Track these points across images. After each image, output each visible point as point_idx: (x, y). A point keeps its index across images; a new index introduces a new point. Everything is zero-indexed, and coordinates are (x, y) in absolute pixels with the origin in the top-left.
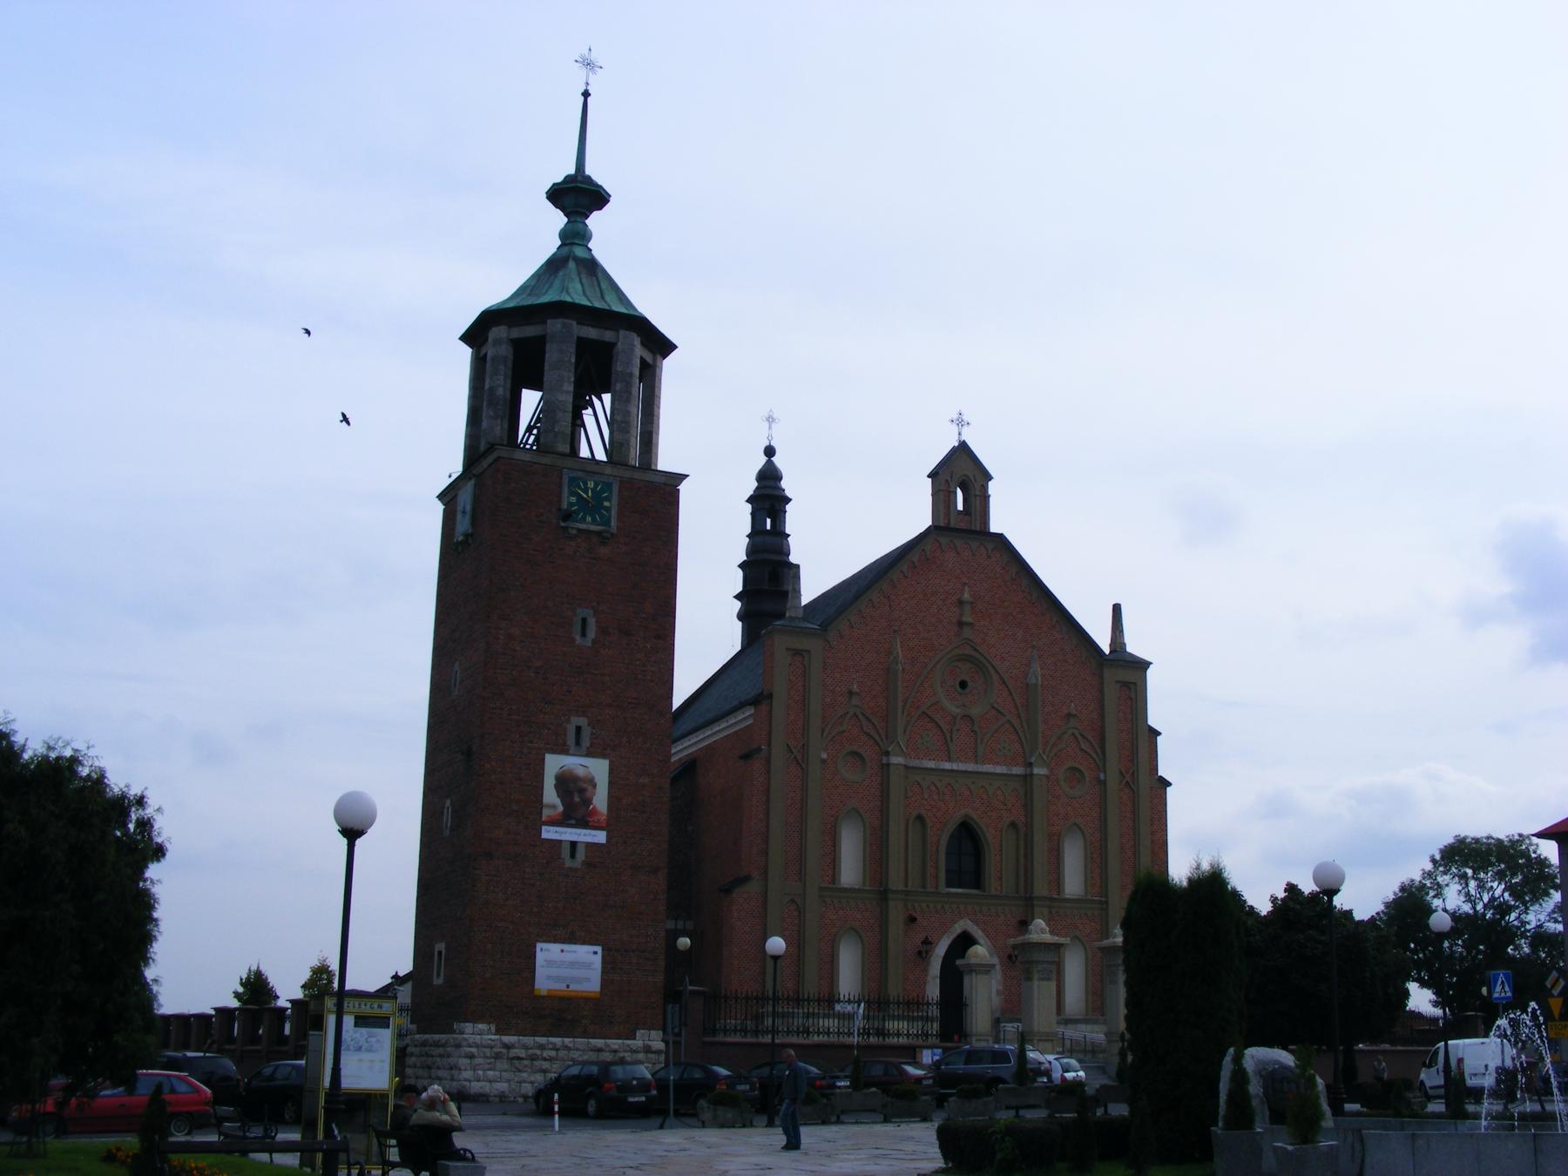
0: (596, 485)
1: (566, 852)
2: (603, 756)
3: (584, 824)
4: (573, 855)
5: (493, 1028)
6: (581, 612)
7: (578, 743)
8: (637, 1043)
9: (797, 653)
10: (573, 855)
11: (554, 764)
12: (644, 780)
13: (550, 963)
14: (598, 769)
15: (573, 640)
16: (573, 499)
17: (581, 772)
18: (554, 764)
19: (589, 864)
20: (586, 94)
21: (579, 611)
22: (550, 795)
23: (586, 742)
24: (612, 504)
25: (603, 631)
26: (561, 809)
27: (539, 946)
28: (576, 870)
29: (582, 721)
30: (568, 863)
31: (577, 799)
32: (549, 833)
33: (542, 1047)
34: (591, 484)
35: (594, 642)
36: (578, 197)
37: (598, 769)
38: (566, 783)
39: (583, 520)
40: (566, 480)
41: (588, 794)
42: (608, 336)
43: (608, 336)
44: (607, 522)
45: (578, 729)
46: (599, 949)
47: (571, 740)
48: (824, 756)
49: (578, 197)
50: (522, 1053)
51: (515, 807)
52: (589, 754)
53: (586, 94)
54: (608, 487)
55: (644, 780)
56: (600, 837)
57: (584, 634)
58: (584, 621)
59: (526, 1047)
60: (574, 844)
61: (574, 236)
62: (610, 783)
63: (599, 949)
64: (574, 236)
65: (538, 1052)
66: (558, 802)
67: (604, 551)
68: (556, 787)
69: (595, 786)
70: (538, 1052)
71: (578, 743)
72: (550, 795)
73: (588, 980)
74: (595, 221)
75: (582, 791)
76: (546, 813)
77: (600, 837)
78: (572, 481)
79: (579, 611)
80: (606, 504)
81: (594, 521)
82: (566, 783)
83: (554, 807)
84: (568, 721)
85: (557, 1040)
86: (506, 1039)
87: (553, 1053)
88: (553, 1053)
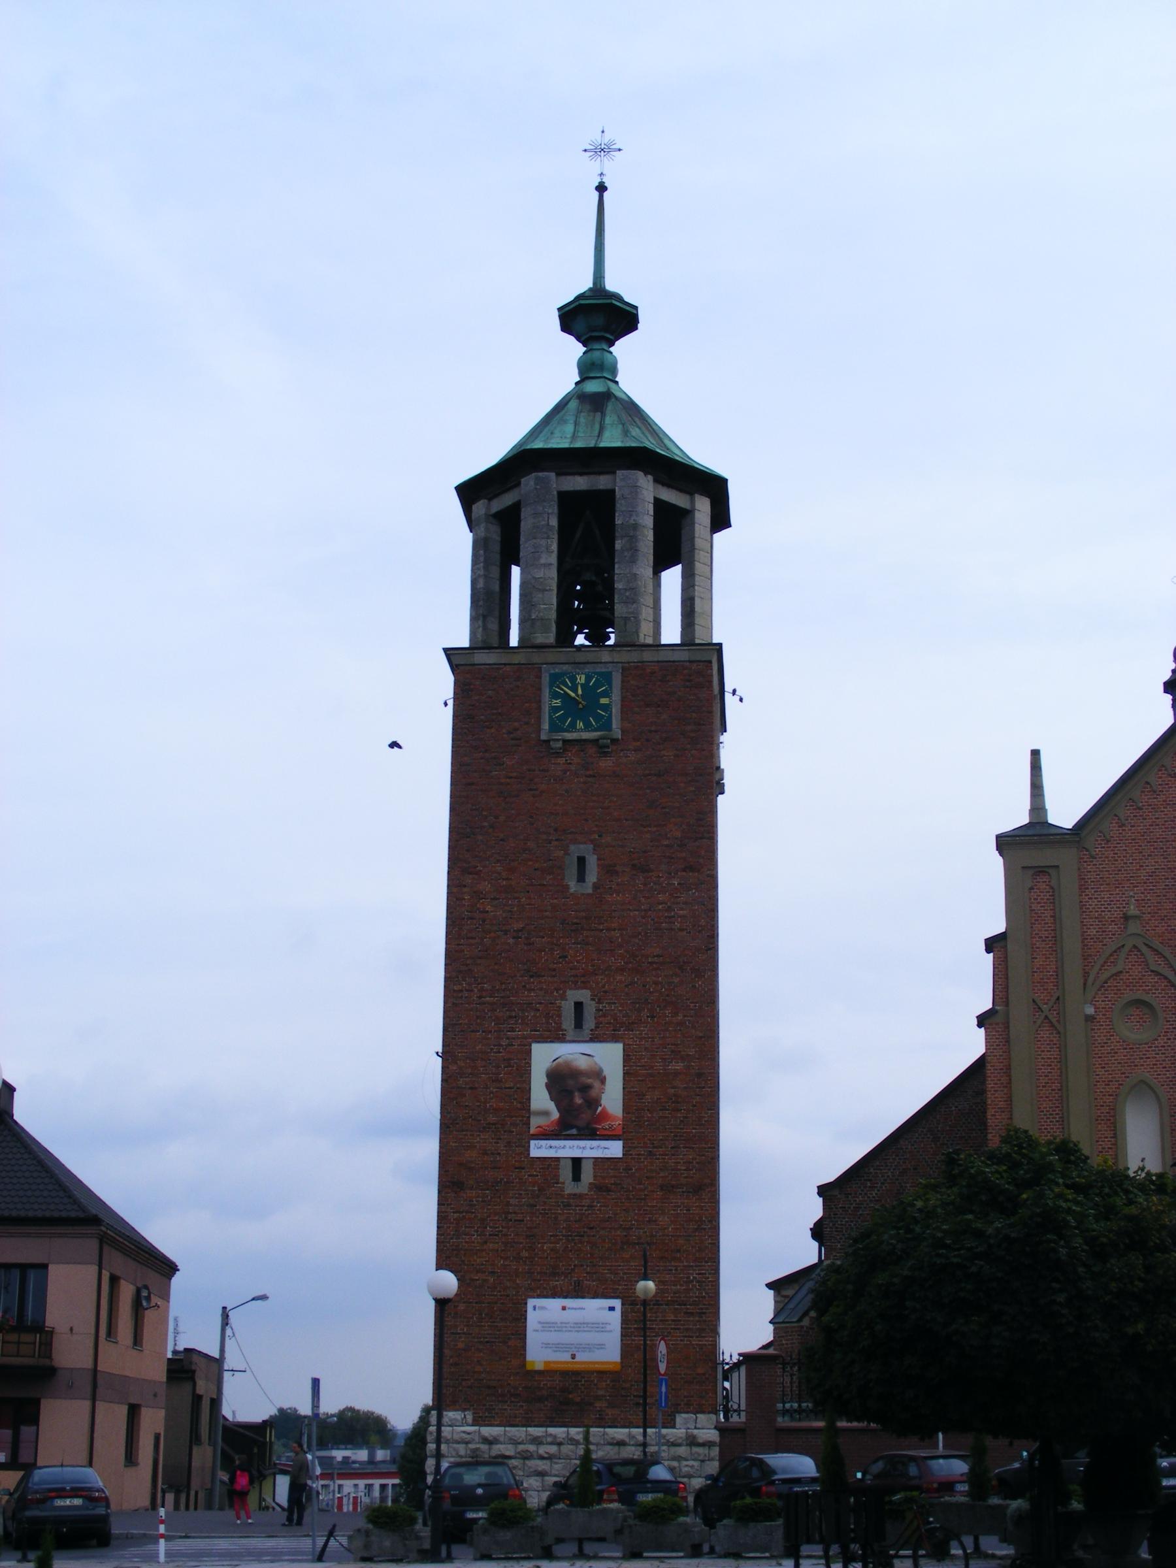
0: (588, 679)
1: (566, 1173)
2: (614, 1039)
3: (590, 1134)
4: (577, 1177)
5: (470, 1418)
6: (576, 850)
7: (579, 1024)
8: (677, 1433)
9: (1041, 871)
10: (577, 1177)
11: (544, 1056)
12: (678, 1066)
13: (547, 1326)
14: (608, 1057)
15: (567, 887)
16: (557, 702)
17: (582, 1063)
18: (544, 1056)
19: (599, 1188)
20: (601, 188)
21: (572, 847)
22: (540, 1098)
23: (589, 1023)
24: (614, 700)
25: (608, 870)
26: (556, 1115)
27: (531, 1302)
28: (580, 1196)
29: (583, 995)
30: (570, 1188)
31: (578, 1100)
32: (540, 1149)
33: (537, 1441)
34: (581, 679)
35: (596, 887)
36: (599, 318)
37: (608, 1057)
38: (563, 1081)
39: (573, 726)
40: (546, 679)
41: (593, 1093)
42: (602, 482)
43: (602, 482)
44: (607, 726)
45: (579, 1006)
46: (617, 1303)
47: (568, 1022)
48: (1090, 1010)
49: (599, 318)
50: (509, 1450)
51: (492, 1118)
52: (594, 1039)
53: (601, 188)
54: (607, 678)
55: (678, 1066)
56: (614, 1149)
57: (581, 878)
58: (582, 861)
59: (515, 1442)
60: (577, 1162)
61: (596, 368)
62: (626, 1074)
63: (617, 1303)
64: (596, 368)
65: (532, 1448)
66: (551, 1106)
67: (606, 764)
68: (548, 1086)
69: (603, 1081)
70: (532, 1448)
71: (579, 1024)
72: (540, 1098)
73: (601, 1346)
74: (623, 349)
75: (585, 1089)
76: (535, 1123)
77: (614, 1149)
78: (555, 679)
79: (572, 847)
80: (604, 701)
81: (588, 727)
82: (563, 1081)
83: (546, 1113)
84: (563, 997)
85: (559, 1432)
86: (487, 1431)
87: (553, 1449)
88: (553, 1449)
